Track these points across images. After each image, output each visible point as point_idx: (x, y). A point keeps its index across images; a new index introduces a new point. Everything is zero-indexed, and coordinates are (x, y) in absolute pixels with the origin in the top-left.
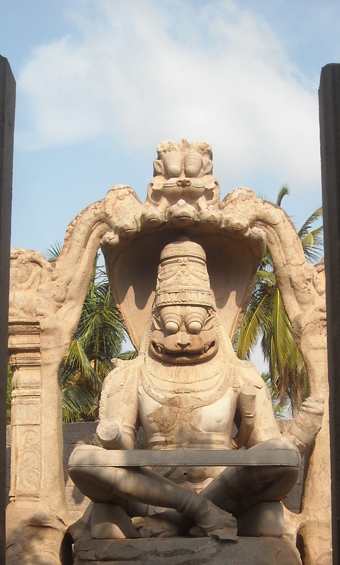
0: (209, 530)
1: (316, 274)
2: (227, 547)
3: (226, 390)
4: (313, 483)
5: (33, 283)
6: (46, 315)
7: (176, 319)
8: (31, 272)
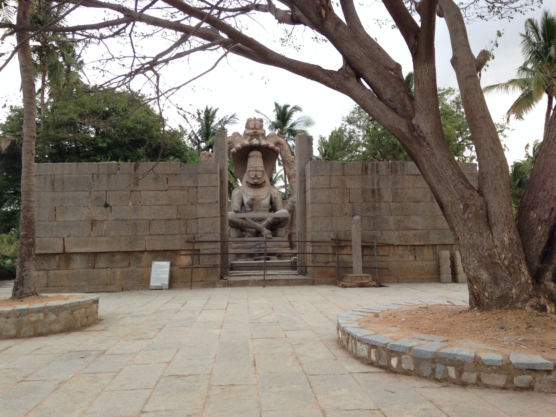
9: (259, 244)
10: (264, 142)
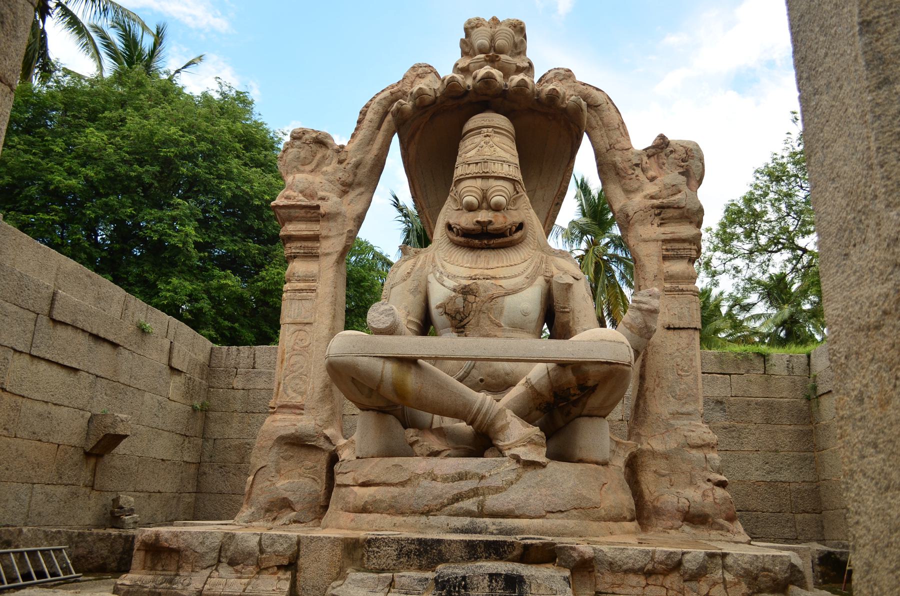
0: (507, 447)
1: (645, 159)
2: (530, 475)
3: (536, 279)
4: (645, 402)
5: (318, 166)
6: (328, 199)
7: (476, 192)
8: (315, 153)
9: (475, 492)
10: (517, 78)
